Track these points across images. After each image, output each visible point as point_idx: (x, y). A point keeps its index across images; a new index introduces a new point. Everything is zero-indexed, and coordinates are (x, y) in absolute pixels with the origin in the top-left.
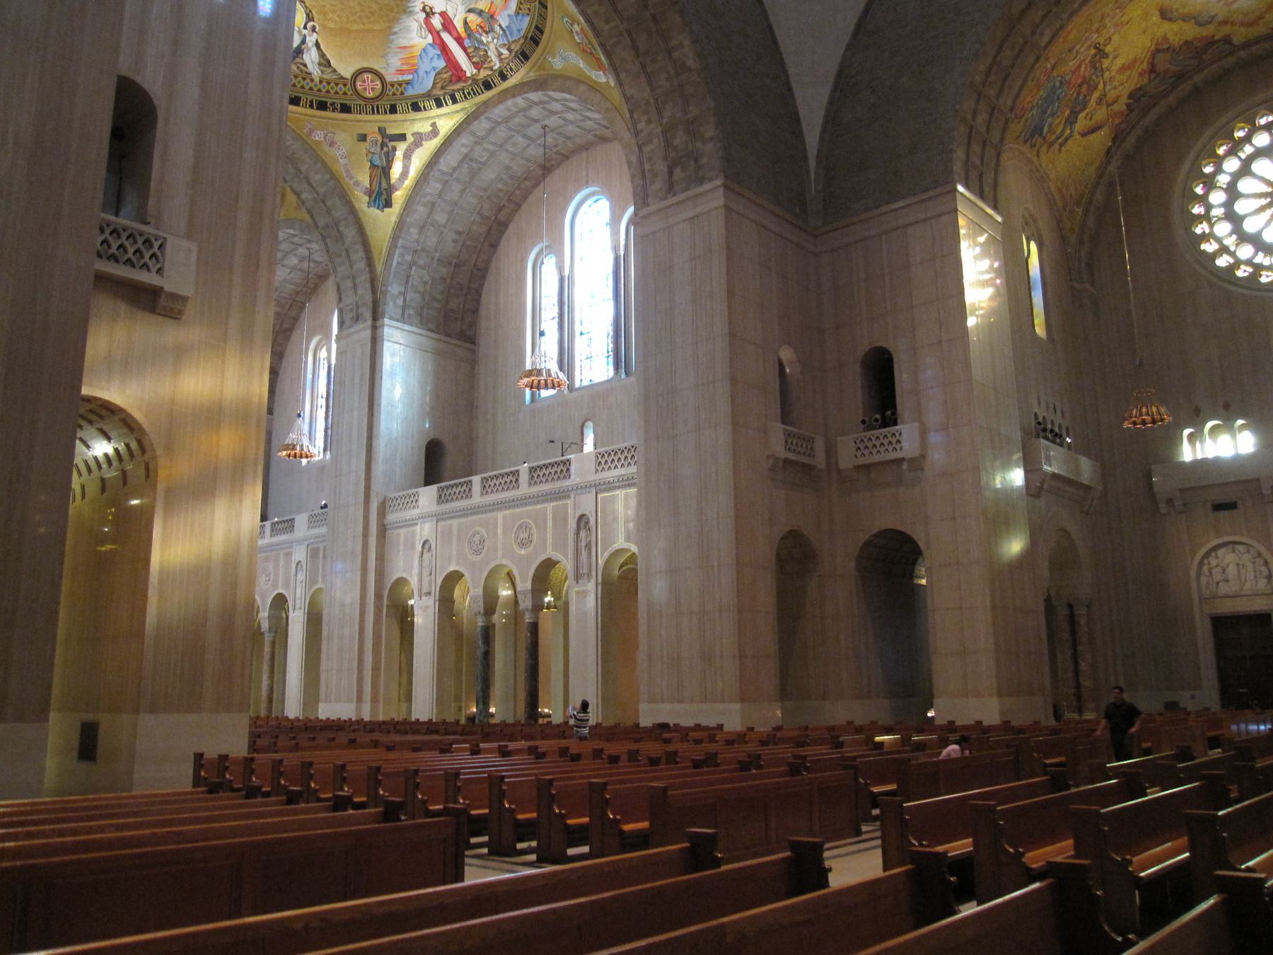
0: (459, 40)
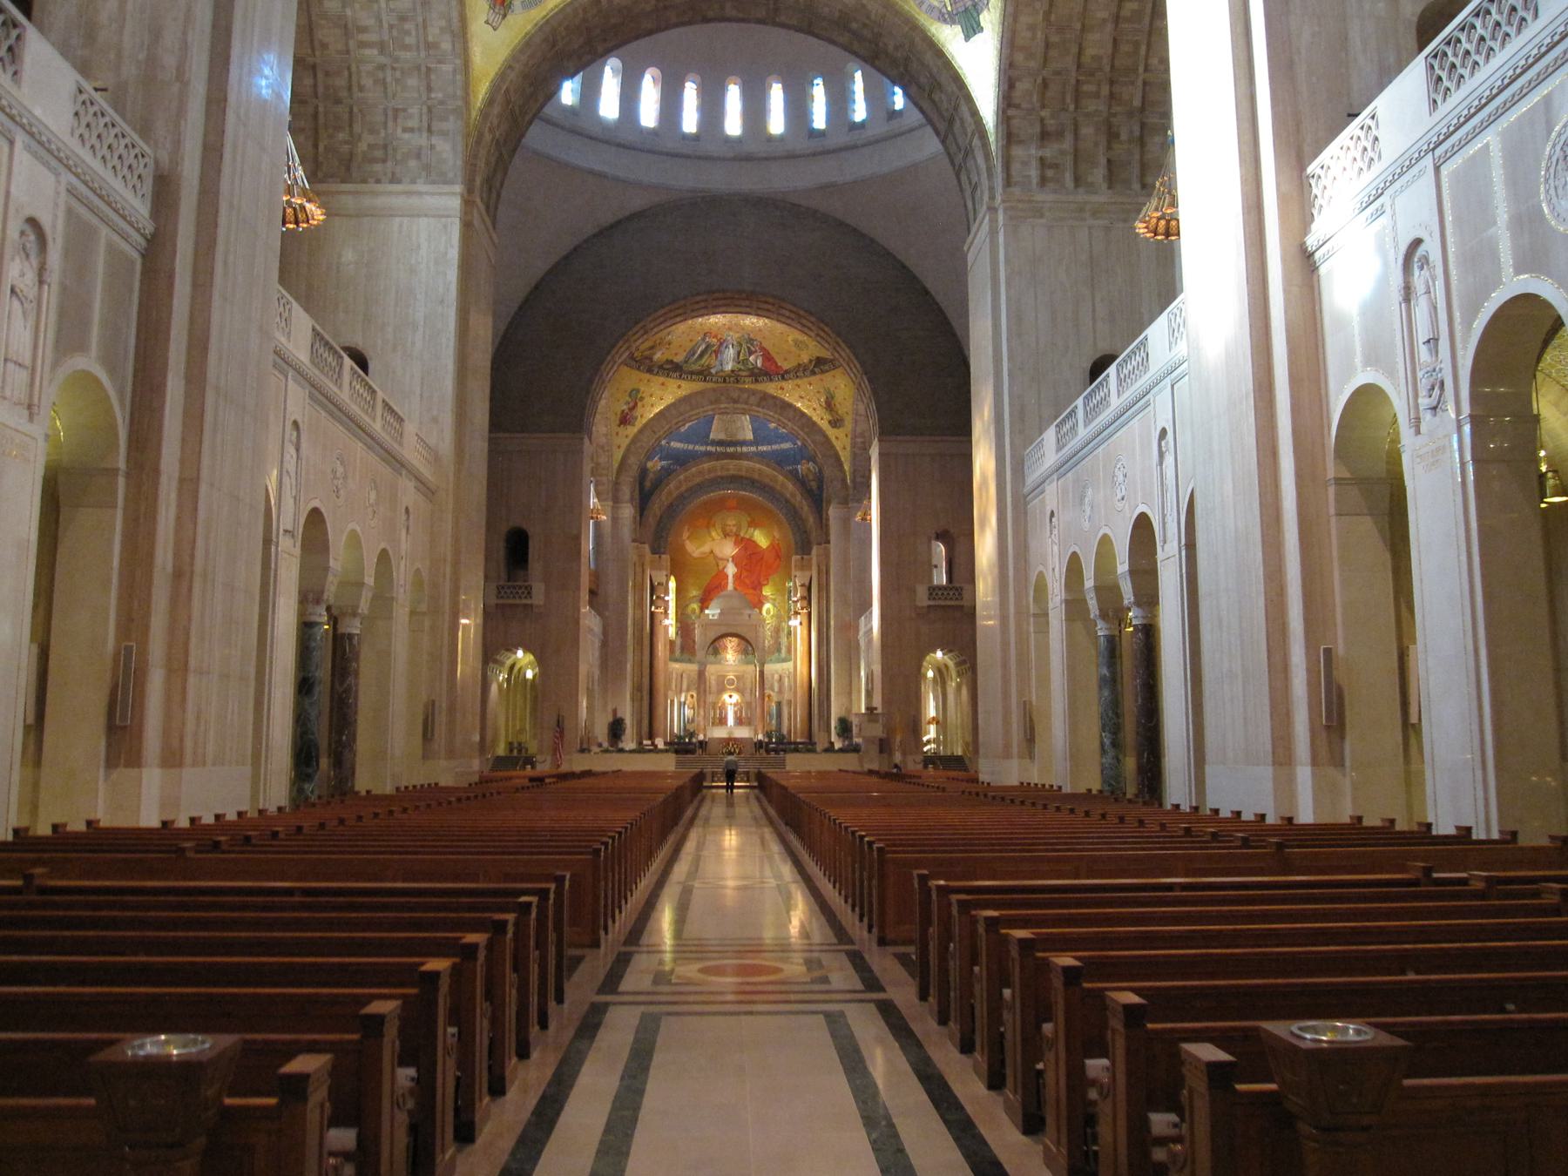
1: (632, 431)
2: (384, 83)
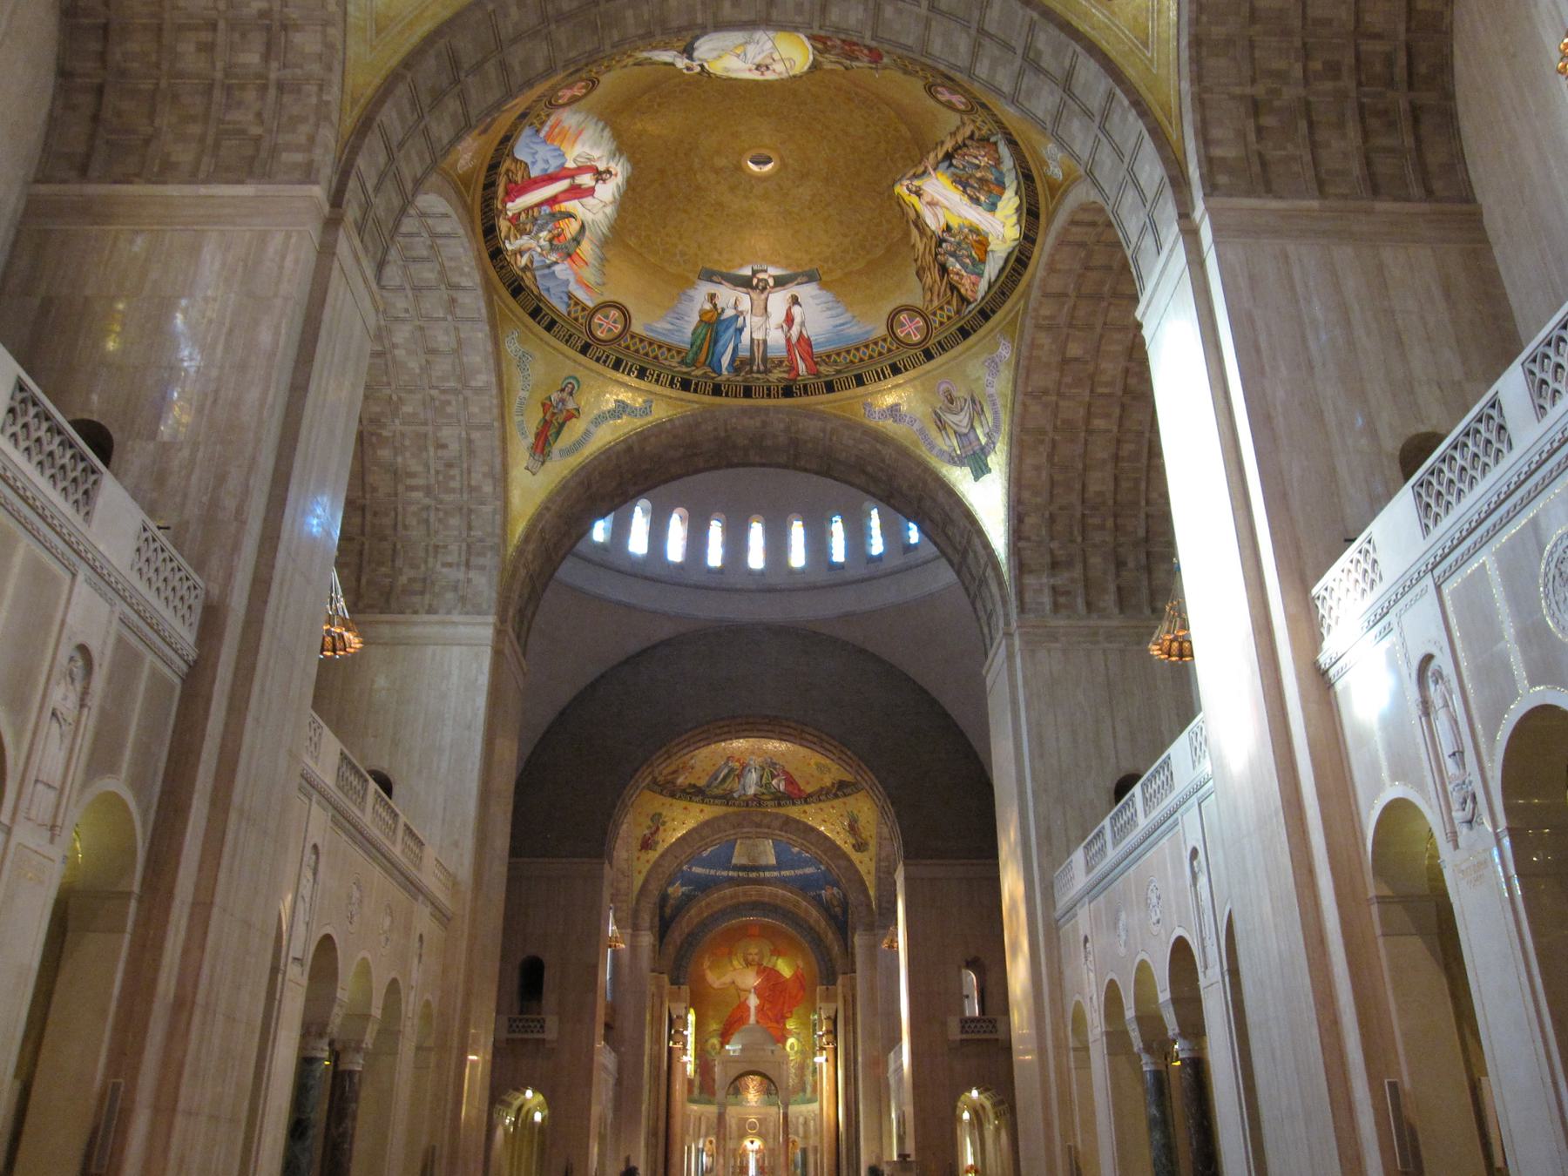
0: (553, 201)
1: (653, 855)
2: (427, 521)
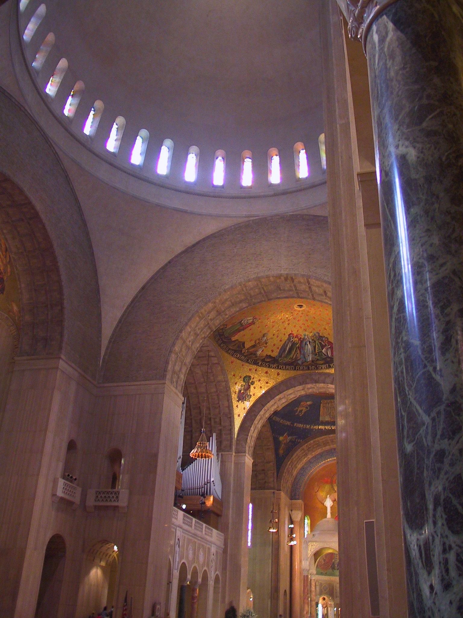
1: (248, 404)
